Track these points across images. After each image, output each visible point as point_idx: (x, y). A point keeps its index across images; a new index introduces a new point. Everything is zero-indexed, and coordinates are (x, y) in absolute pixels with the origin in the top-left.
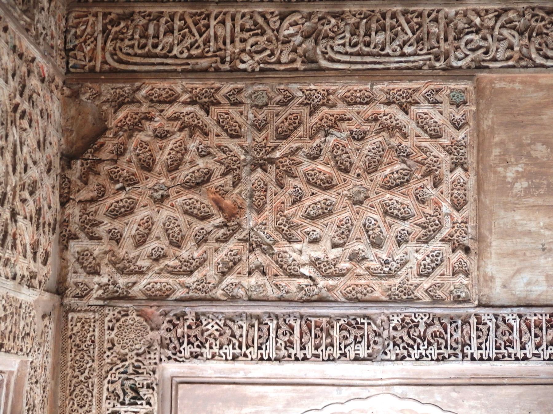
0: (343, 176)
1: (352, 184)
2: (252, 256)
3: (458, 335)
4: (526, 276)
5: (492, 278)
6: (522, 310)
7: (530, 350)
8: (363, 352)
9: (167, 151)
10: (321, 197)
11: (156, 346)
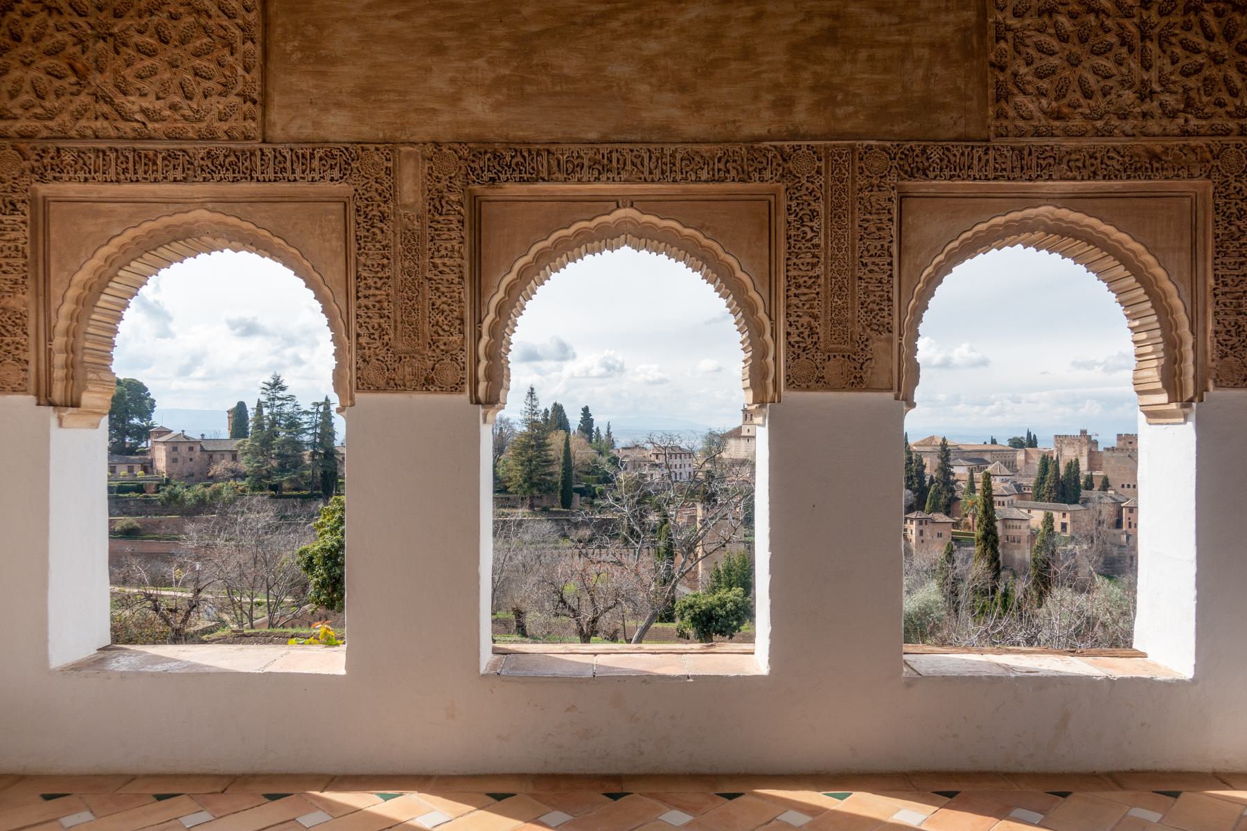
0: (165, 46)
1: (172, 52)
2: (97, 106)
3: (247, 164)
4: (298, 122)
5: (275, 124)
6: (293, 146)
7: (298, 174)
8: (179, 177)
9: (33, 26)
10: (148, 62)
11: (28, 172)
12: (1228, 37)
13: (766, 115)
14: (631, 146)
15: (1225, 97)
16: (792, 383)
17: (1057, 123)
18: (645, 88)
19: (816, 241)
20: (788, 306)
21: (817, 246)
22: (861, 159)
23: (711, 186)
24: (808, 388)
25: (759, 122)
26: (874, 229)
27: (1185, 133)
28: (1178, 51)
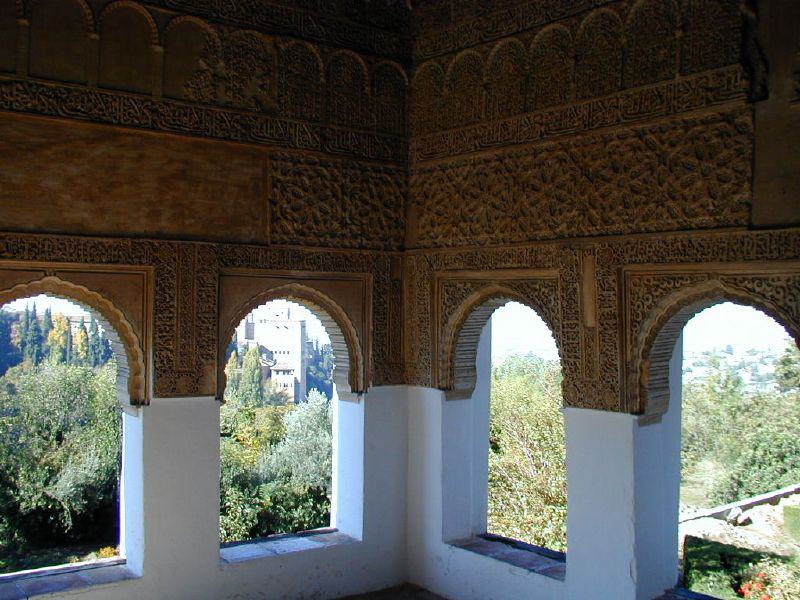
12: (380, 197)
13: (143, 221)
14: (58, 237)
15: (380, 230)
16: (156, 395)
17: (302, 237)
18: (67, 197)
19: (171, 303)
20: (155, 344)
21: (173, 306)
22: (199, 253)
23: (109, 265)
24: (167, 396)
25: (142, 225)
26: (204, 296)
27: (362, 247)
28: (359, 203)
